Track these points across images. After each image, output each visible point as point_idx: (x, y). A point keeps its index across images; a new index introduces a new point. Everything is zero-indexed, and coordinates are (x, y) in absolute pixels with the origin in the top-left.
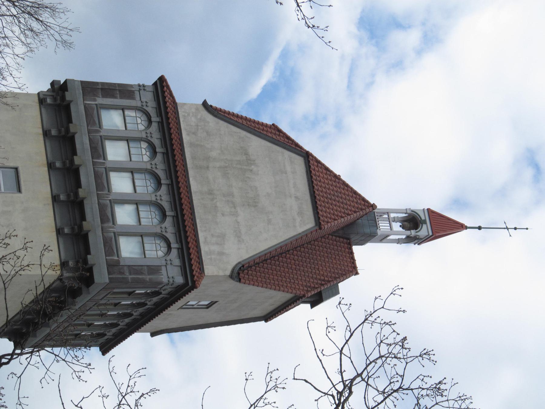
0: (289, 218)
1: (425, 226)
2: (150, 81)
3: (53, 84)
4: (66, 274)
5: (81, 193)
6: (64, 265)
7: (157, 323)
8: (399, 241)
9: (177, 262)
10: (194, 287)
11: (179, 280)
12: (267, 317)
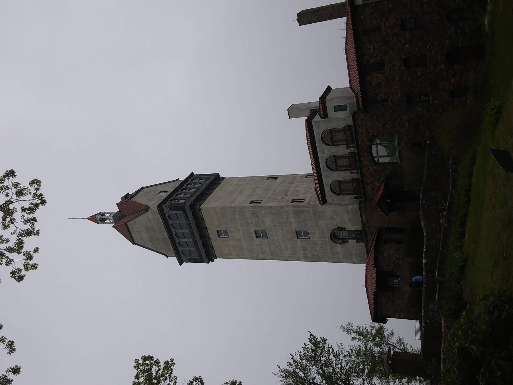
0: (137, 224)
1: (99, 219)
2: (184, 263)
3: (213, 261)
4: (198, 207)
5: (198, 232)
6: (200, 210)
7: (177, 184)
8: (107, 213)
9: (165, 212)
10: (158, 206)
11: (163, 206)
12: (143, 188)
